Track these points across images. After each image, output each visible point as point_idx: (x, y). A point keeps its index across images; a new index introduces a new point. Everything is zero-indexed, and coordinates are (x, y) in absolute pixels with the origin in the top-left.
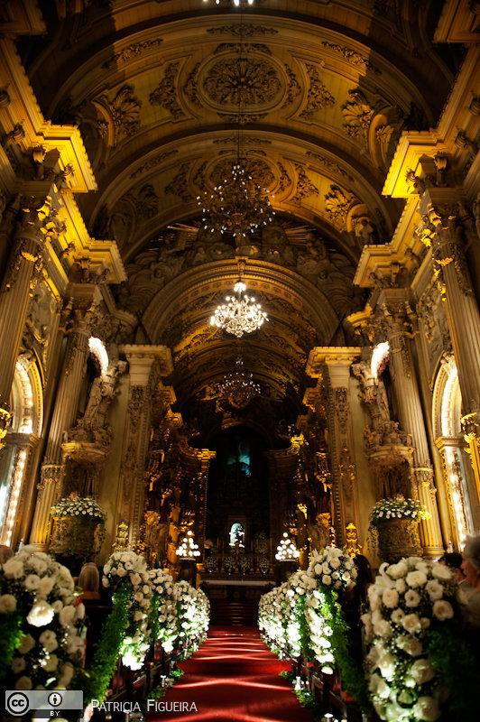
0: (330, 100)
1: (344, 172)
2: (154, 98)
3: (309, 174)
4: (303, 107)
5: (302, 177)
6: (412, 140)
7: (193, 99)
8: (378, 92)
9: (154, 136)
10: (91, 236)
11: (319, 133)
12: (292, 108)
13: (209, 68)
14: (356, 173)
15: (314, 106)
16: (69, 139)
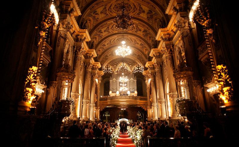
0: (144, 12)
1: (147, 28)
2: (101, 13)
3: (139, 26)
4: (137, 13)
5: (137, 27)
6: (162, 30)
7: (111, 11)
8: (155, 11)
9: (101, 21)
10: (89, 48)
11: (142, 18)
12: (134, 13)
13: (114, 5)
14: (150, 29)
15: (140, 13)
16: (85, 32)
